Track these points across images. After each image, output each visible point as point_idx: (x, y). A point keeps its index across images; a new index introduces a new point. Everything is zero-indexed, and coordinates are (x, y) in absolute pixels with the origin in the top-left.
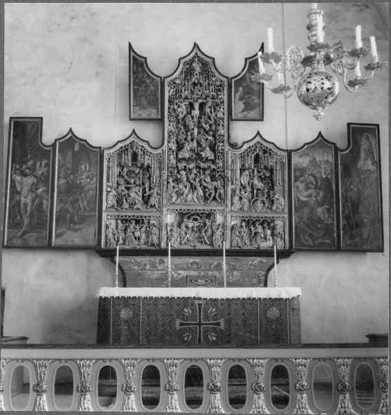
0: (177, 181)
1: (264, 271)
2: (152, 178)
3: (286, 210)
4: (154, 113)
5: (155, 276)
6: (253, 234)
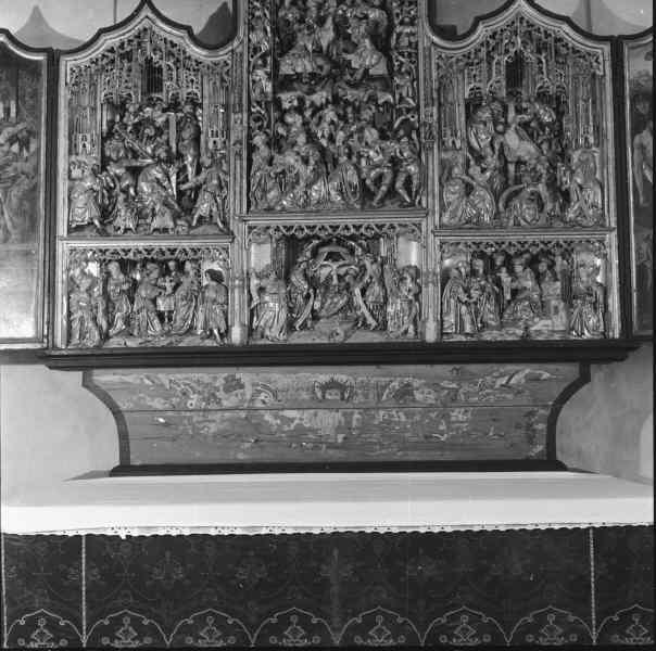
0: (276, 143)
2: (202, 137)
3: (612, 221)
5: (213, 428)
6: (508, 297)
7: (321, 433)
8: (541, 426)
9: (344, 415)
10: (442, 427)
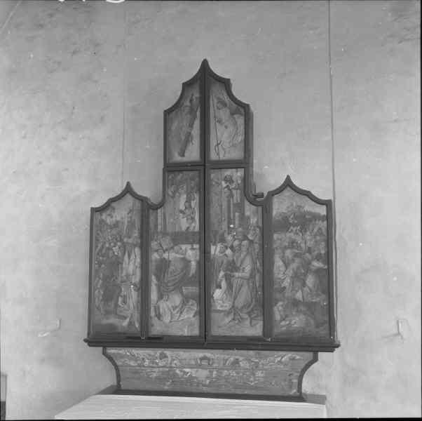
1: (298, 372)
5: (155, 375)
7: (200, 379)
8: (295, 381)
9: (210, 371)
10: (252, 379)
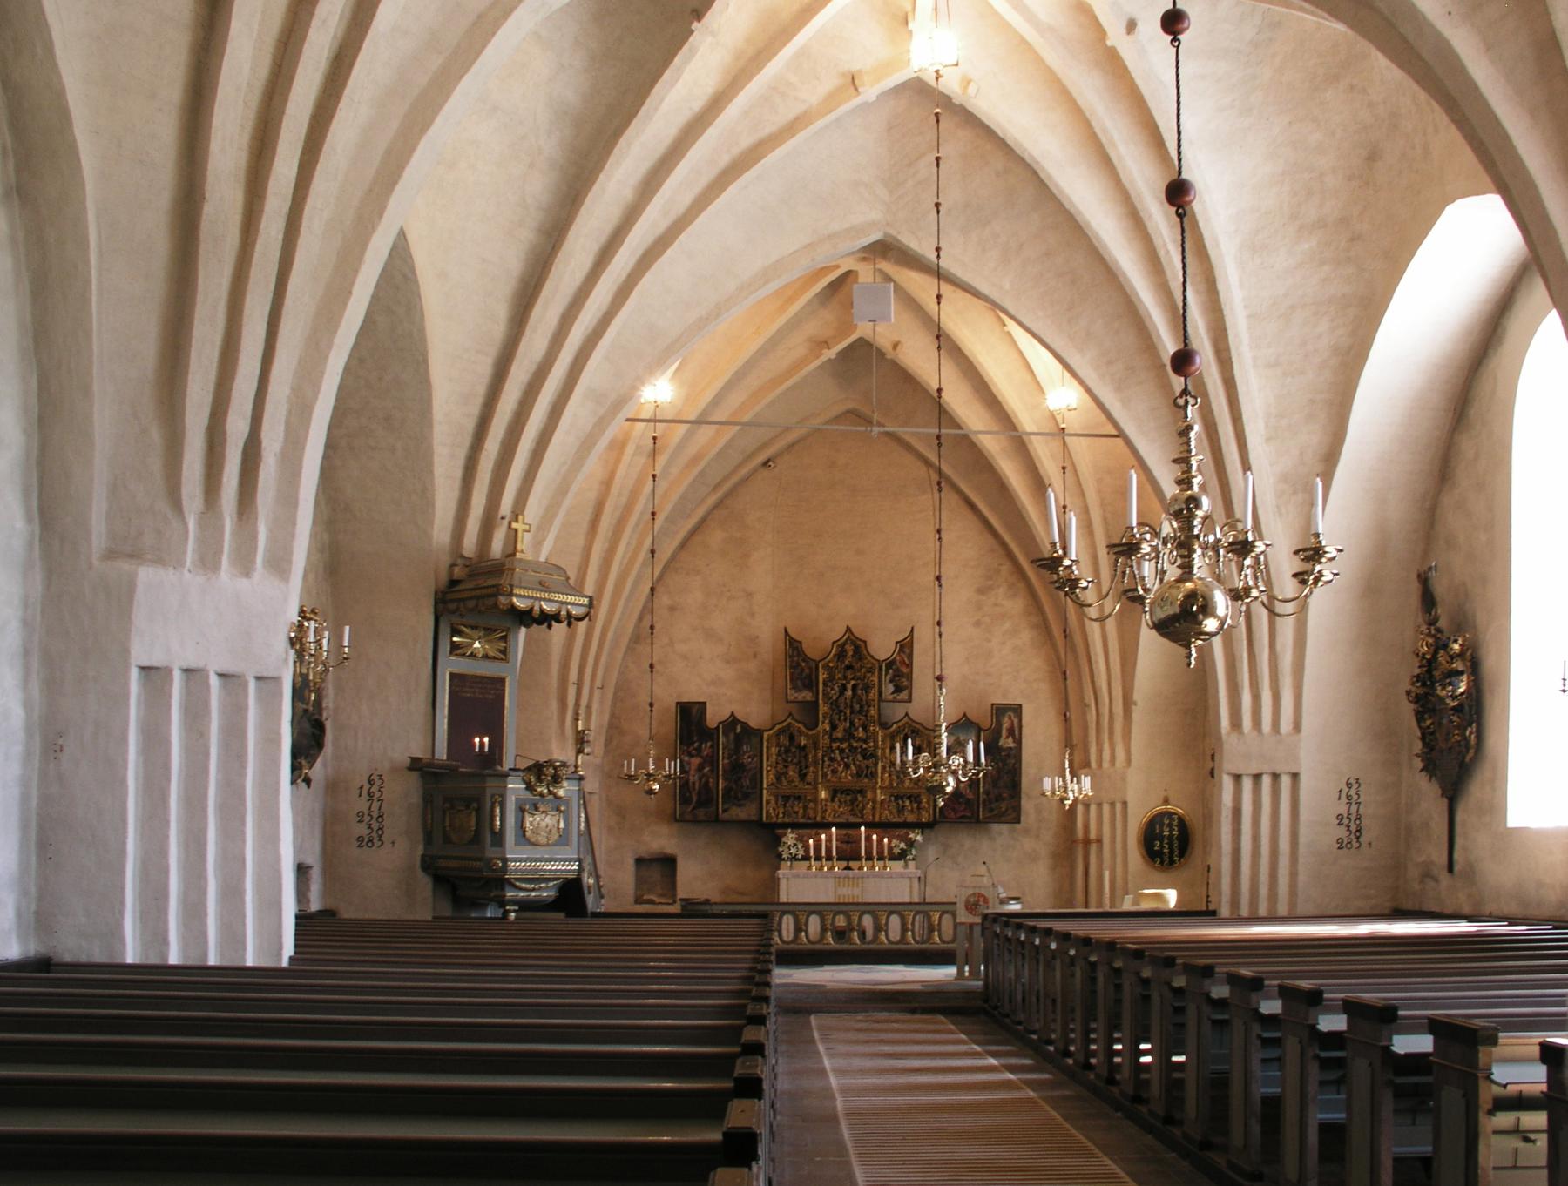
0: (832, 759)
4: (808, 696)
